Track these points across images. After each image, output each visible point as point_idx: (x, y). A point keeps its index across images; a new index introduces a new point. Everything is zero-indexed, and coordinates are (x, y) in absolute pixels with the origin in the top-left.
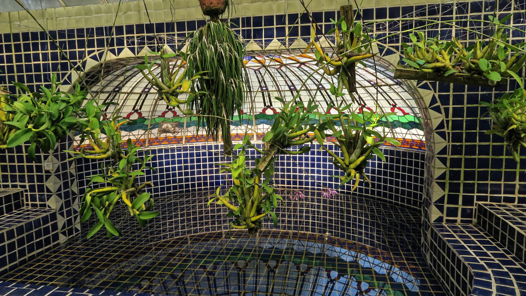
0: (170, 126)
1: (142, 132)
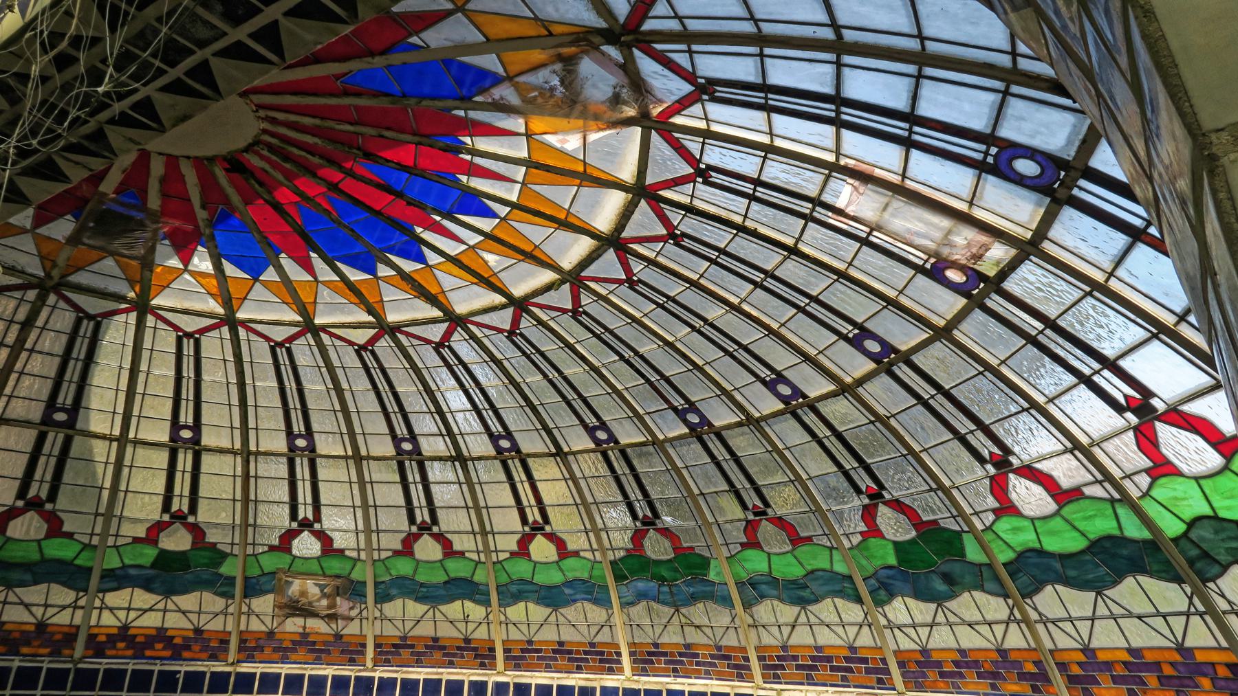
0: (312, 588)
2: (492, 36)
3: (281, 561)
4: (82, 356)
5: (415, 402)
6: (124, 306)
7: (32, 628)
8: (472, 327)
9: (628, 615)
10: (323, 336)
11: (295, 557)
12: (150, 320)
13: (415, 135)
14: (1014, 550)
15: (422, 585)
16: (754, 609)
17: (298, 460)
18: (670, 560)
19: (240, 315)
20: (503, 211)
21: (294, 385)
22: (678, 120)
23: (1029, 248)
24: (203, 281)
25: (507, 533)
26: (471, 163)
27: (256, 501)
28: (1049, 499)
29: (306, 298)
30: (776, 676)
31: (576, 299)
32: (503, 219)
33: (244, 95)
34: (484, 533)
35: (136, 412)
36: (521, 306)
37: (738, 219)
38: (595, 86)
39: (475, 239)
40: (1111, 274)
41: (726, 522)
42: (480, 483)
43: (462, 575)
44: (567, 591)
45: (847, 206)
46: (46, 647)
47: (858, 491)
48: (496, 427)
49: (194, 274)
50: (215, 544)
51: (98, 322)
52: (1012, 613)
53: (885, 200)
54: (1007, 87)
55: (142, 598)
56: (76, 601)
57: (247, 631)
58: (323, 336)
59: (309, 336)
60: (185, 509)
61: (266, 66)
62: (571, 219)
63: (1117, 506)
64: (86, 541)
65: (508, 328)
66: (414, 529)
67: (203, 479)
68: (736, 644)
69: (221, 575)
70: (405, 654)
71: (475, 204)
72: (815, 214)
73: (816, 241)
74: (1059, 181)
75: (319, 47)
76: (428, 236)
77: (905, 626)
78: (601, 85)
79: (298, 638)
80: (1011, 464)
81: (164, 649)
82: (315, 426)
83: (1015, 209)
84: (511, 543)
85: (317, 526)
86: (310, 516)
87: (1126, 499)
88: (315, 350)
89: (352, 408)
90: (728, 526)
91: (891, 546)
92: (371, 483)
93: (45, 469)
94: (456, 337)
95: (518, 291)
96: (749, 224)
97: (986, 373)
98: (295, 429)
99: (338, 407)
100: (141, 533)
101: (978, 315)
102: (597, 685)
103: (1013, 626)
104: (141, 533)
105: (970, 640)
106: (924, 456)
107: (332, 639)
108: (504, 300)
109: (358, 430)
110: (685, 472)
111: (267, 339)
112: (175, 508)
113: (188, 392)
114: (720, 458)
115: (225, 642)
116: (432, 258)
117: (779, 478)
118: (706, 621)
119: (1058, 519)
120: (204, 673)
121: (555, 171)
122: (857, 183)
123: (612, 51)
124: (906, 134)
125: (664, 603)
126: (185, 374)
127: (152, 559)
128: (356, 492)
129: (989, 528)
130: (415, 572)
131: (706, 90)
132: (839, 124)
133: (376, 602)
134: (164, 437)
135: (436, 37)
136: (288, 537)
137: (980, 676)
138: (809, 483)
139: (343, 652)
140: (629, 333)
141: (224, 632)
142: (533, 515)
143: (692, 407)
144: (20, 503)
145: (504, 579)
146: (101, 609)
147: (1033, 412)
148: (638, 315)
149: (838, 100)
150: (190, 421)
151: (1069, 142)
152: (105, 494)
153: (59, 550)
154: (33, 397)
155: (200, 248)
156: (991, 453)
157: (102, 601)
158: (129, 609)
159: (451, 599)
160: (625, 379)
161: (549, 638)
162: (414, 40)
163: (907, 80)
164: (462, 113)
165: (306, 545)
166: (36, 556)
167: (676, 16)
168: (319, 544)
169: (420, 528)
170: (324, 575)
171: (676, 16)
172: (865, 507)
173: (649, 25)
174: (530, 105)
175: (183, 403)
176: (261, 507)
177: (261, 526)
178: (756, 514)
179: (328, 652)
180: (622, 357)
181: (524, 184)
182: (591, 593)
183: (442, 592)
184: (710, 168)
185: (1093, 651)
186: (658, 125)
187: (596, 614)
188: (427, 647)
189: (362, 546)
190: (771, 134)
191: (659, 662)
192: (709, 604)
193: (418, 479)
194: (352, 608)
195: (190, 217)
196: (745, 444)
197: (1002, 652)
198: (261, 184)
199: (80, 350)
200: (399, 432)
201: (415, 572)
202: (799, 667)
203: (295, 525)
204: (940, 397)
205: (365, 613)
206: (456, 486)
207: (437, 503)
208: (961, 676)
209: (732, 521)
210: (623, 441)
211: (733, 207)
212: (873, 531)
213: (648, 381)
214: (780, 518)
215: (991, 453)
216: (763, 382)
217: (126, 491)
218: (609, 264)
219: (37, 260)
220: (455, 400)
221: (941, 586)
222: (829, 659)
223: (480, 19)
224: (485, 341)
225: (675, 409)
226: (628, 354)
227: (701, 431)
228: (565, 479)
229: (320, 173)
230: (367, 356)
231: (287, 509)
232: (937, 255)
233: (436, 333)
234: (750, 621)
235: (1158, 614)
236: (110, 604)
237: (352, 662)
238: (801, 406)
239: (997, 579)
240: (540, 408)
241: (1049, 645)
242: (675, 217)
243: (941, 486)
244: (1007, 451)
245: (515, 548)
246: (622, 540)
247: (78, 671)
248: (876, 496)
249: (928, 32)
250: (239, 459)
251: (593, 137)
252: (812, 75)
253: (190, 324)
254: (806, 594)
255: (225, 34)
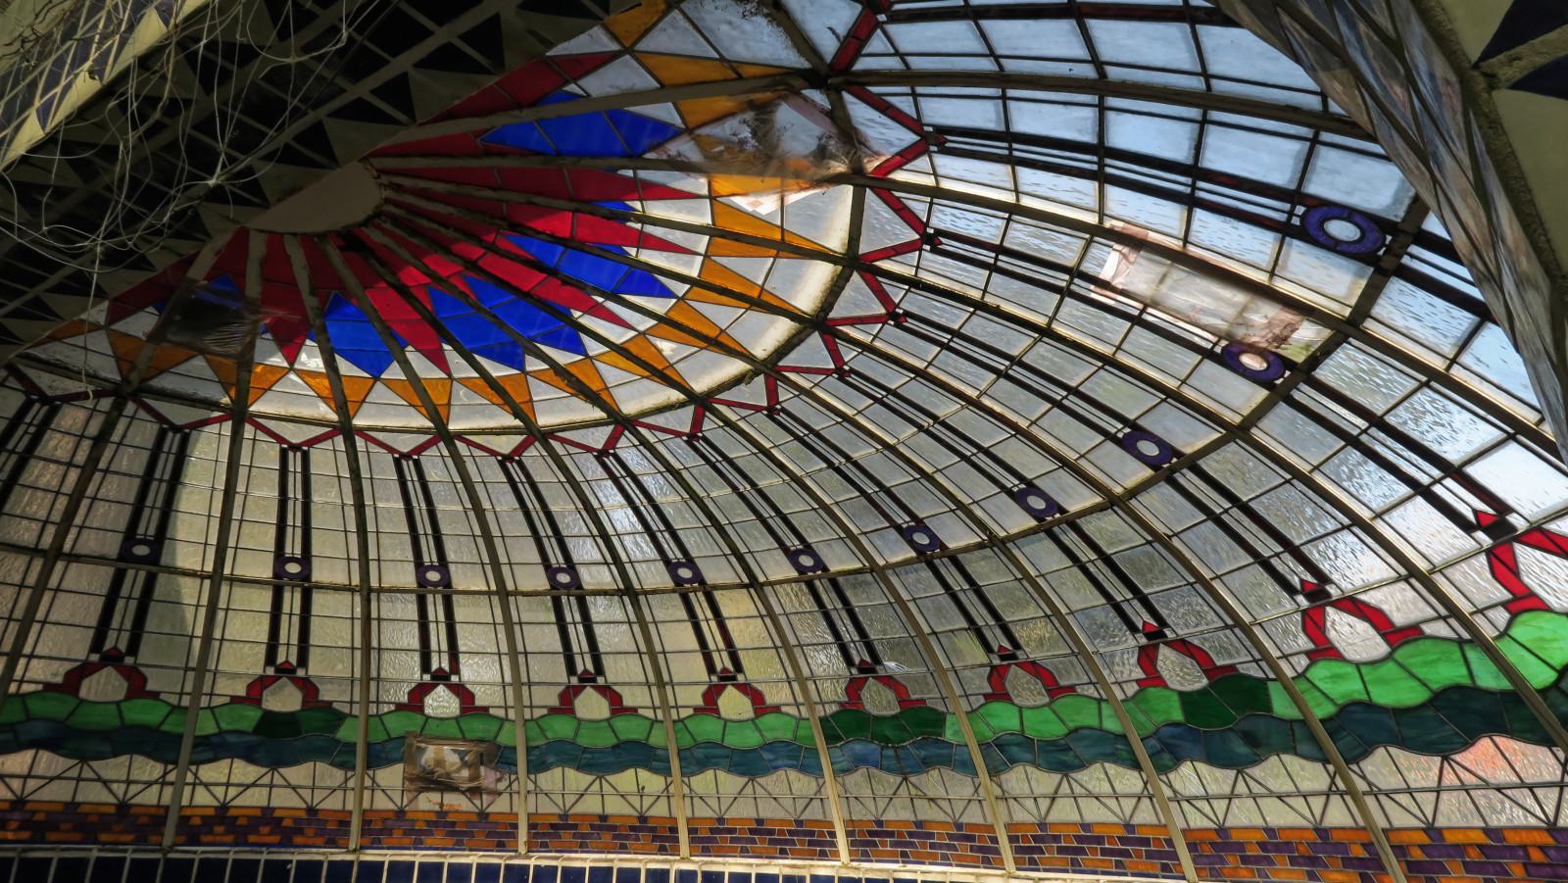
0: (450, 756)
1: (329, 774)
2: (667, 82)
3: (412, 722)
4: (167, 477)
5: (573, 523)
6: (216, 414)
7: (112, 810)
8: (642, 430)
9: (844, 786)
10: (461, 446)
11: (428, 717)
12: (249, 431)
13: (571, 200)
14: (1335, 704)
15: (585, 750)
16: (1003, 777)
17: (430, 598)
18: (894, 717)
19: (358, 422)
20: (681, 289)
21: (424, 506)
22: (899, 176)
23: (1348, 329)
24: (312, 382)
25: (690, 684)
26: (641, 232)
27: (379, 649)
28: (1379, 639)
29: (439, 400)
30: (1032, 862)
31: (772, 394)
32: (682, 299)
33: (364, 160)
34: (661, 684)
35: (232, 543)
36: (703, 403)
37: (976, 295)
38: (795, 138)
39: (645, 324)
40: (1453, 361)
41: (965, 668)
42: (655, 623)
43: (634, 736)
44: (767, 756)
45: (1114, 277)
46: (129, 833)
47: (1133, 628)
48: (673, 553)
49: (304, 374)
50: (331, 703)
51: (185, 434)
52: (1333, 782)
53: (1163, 269)
54: (1316, 135)
55: (244, 771)
56: (164, 776)
57: (371, 811)
58: (461, 446)
59: (441, 444)
60: (293, 660)
61: (391, 127)
62: (765, 298)
63: (1467, 648)
64: (176, 703)
65: (687, 430)
66: (574, 681)
67: (315, 623)
68: (980, 820)
69: (338, 742)
70: (566, 836)
71: (649, 281)
72: (1073, 287)
73: (1074, 319)
74: (1383, 249)
75: (457, 102)
76: (587, 321)
77: (1196, 798)
78: (803, 137)
79: (433, 818)
80: (1328, 595)
81: (270, 834)
82: (451, 556)
83: (1330, 281)
84: (694, 697)
85: (454, 679)
86: (447, 668)
87: (1478, 639)
88: (450, 462)
89: (495, 532)
90: (967, 673)
91: (1175, 697)
92: (520, 624)
93: (123, 615)
94: (623, 442)
95: (700, 386)
96: (989, 300)
97: (1295, 482)
98: (426, 559)
99: (478, 532)
100: (242, 692)
101: (1283, 409)
102: (806, 873)
103: (1335, 799)
104: (242, 692)
105: (1279, 816)
106: (1216, 584)
107: (475, 818)
108: (682, 397)
109: (503, 559)
110: (912, 606)
111: (391, 450)
112: (281, 659)
113: (294, 517)
114: (957, 588)
115: (345, 824)
116: (594, 348)
117: (1032, 611)
118: (940, 792)
119: (1390, 666)
120: (320, 863)
121: (745, 243)
122: (1126, 250)
123: (817, 96)
124: (1188, 190)
125: (889, 770)
126: (291, 495)
127: (253, 724)
128: (502, 635)
129: (1302, 676)
130: (576, 734)
131: (935, 139)
132: (1102, 178)
133: (529, 772)
134: (266, 573)
135: (597, 85)
136: (420, 692)
137: (1293, 861)
138: (1069, 618)
139: (489, 835)
140: (839, 435)
141: (343, 811)
142: (722, 661)
143: (920, 525)
144: (95, 657)
145: (687, 741)
146: (194, 785)
147: (1356, 529)
148: (850, 412)
149: (1101, 149)
150: (298, 551)
151: (1396, 200)
152: (197, 643)
153: (143, 713)
154: (108, 527)
155: (308, 342)
156: (1302, 581)
157: (196, 775)
158: (228, 785)
159: (621, 767)
160: (833, 491)
161: (745, 816)
162: (572, 88)
163: (1188, 126)
164: (630, 173)
165: (441, 703)
166: (115, 722)
167: (897, 53)
168: (457, 701)
169: (581, 680)
170: (464, 739)
171: (897, 53)
172: (1142, 649)
173: (863, 64)
174: (718, 161)
175: (289, 530)
176: (385, 656)
177: (386, 680)
178: (1002, 658)
179: (471, 835)
180: (830, 464)
181: (706, 256)
182: (796, 758)
183: (611, 759)
184: (940, 233)
185: (1440, 831)
186: (874, 184)
187: (802, 783)
188: (593, 827)
189: (511, 702)
190: (1017, 191)
191: (884, 844)
192: (947, 773)
193: (578, 618)
194: (499, 780)
195: (298, 306)
196: (989, 572)
197: (1322, 832)
198: (383, 264)
199: (164, 469)
200: (553, 561)
201: (576, 734)
202: (1061, 850)
203: (427, 678)
204: (1235, 512)
205: (515, 786)
206: (625, 627)
207: (602, 648)
208: (1270, 861)
209: (973, 667)
210: (834, 568)
211: (969, 280)
212: (1152, 678)
213: (863, 492)
214: (1034, 663)
215: (1302, 581)
216: (1009, 492)
217: (222, 640)
218: (814, 351)
219: (112, 362)
220: (621, 518)
221: (1242, 749)
222: (1099, 840)
223: (651, 61)
224: (660, 448)
225: (898, 528)
226: (838, 460)
227: (932, 555)
228: (762, 617)
229: (457, 248)
230: (513, 468)
231: (417, 657)
232: (1229, 336)
233: (598, 438)
234: (998, 792)
235: (1523, 785)
236: (204, 780)
237: (501, 847)
238: (1058, 523)
239: (1313, 739)
240: (729, 529)
241: (1382, 823)
242: (896, 293)
243: (1238, 622)
244: (1323, 579)
245: (700, 702)
246: (833, 692)
247: (168, 861)
248: (1156, 635)
249: (1214, 68)
250: (358, 598)
251: (793, 198)
252: (1070, 121)
253: (296, 434)
254: (1068, 758)
255: (343, 91)
